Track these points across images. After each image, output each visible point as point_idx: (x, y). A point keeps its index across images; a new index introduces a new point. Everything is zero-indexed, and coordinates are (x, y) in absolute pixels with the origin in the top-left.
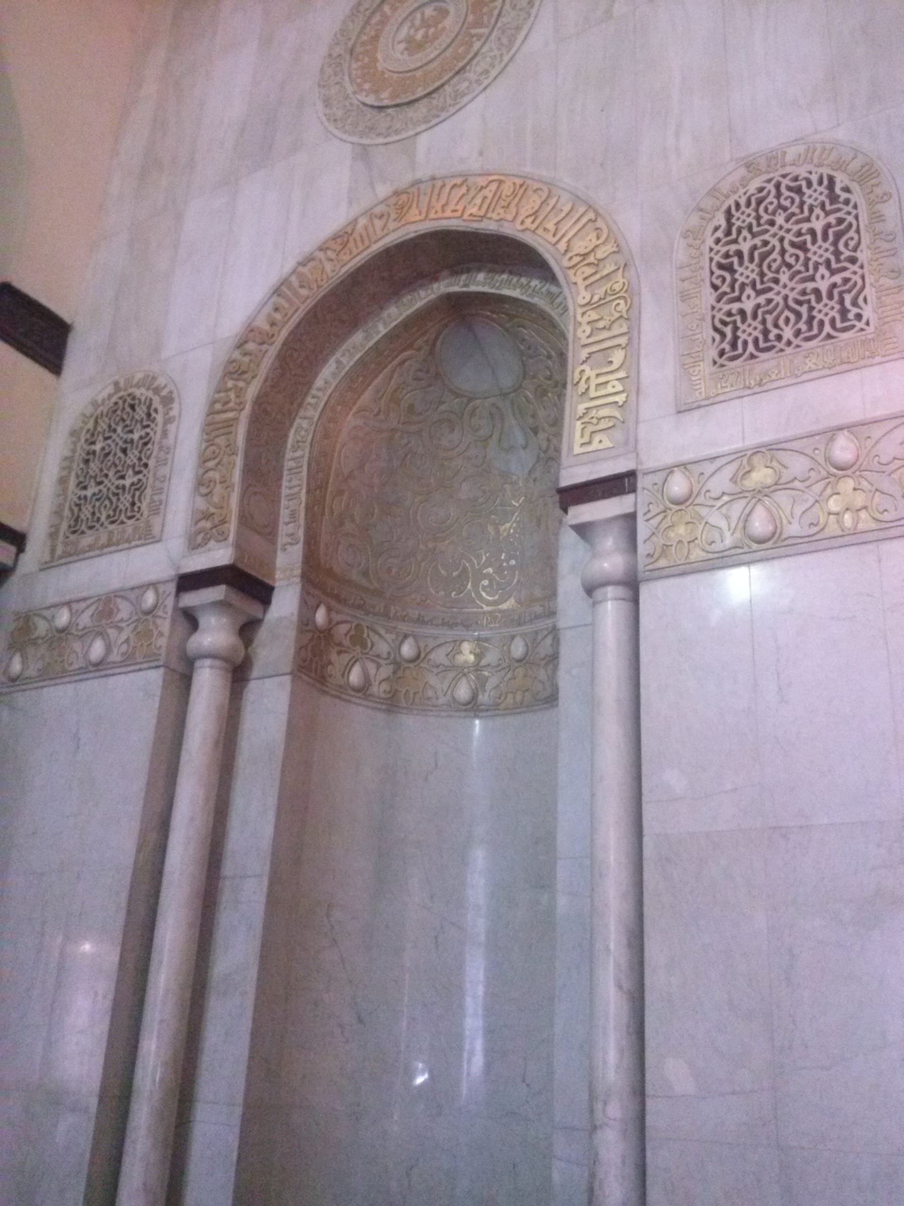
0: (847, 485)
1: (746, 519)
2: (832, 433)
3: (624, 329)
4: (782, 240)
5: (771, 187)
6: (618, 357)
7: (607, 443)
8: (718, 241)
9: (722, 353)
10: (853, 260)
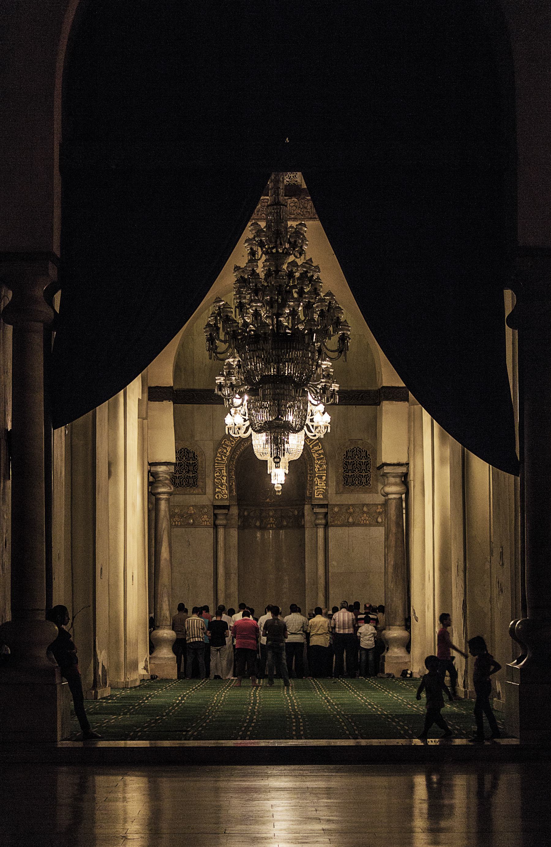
0: (365, 515)
1: (348, 519)
2: (363, 505)
3: (325, 472)
4: (357, 462)
5: (355, 449)
6: (324, 478)
7: (322, 497)
8: (344, 458)
9: (345, 483)
10: (369, 471)
